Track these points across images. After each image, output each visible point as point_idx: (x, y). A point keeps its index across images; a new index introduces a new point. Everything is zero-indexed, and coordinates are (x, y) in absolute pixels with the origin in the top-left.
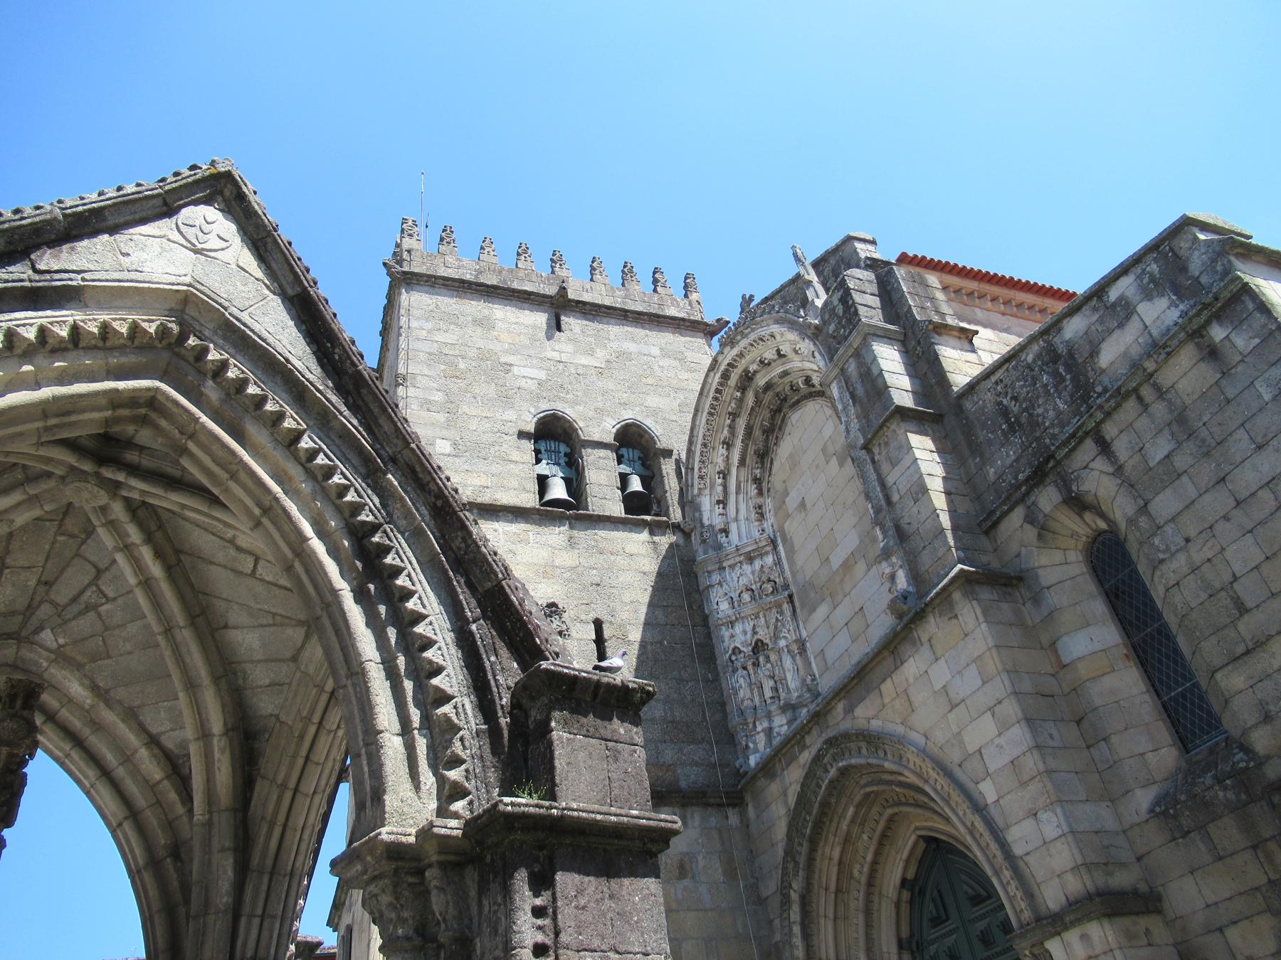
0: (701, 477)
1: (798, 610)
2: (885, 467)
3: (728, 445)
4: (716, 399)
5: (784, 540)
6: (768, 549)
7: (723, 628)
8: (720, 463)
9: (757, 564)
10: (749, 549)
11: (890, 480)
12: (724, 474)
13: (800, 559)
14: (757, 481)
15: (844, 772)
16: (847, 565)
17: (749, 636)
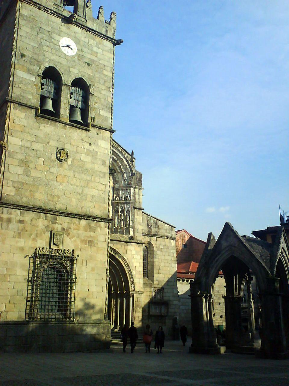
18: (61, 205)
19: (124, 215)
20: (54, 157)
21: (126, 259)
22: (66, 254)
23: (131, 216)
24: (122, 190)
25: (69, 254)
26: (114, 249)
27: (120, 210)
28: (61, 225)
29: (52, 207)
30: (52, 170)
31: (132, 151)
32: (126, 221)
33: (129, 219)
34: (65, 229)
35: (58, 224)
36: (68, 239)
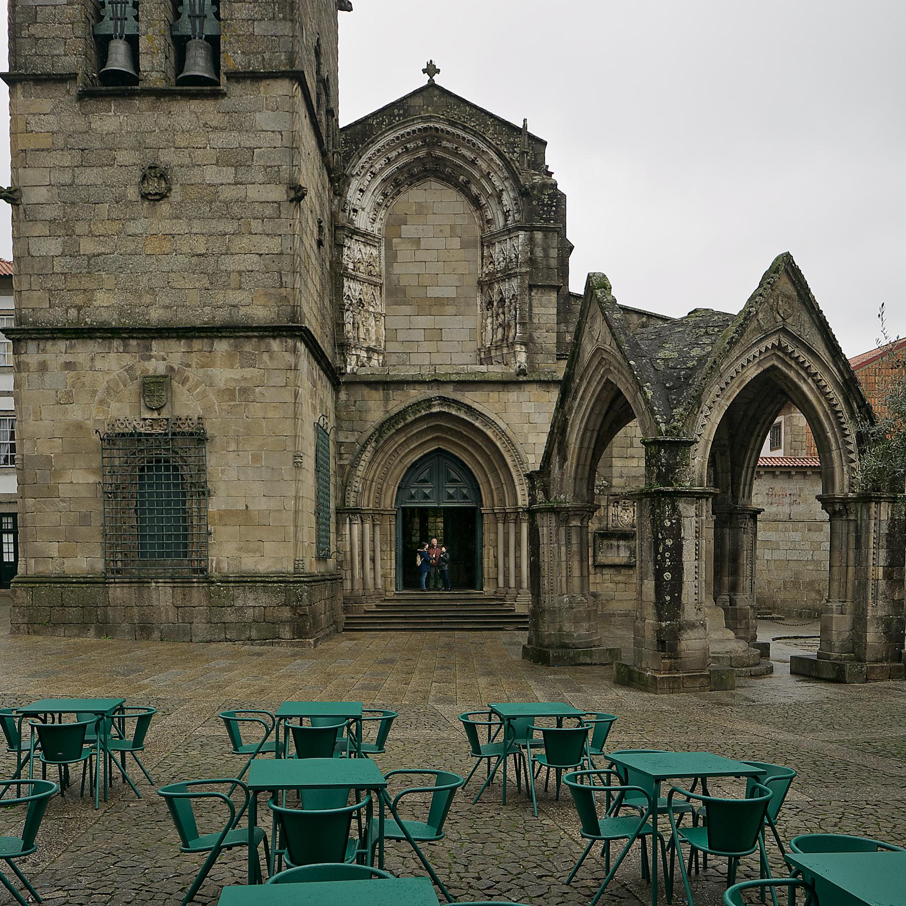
0: (363, 167)
1: (383, 296)
2: (535, 303)
3: (389, 162)
4: (408, 133)
5: (389, 246)
6: (376, 244)
7: (345, 279)
8: (378, 166)
9: (369, 250)
10: (369, 237)
11: (536, 311)
12: (374, 175)
13: (397, 269)
14: (385, 195)
15: (441, 413)
16: (440, 302)
17: (357, 294)
18: (161, 311)
19: (504, 313)
20: (132, 193)
21: (503, 426)
22: (179, 427)
23: (518, 312)
24: (499, 242)
25: (189, 426)
26: (468, 406)
27: (496, 298)
28: (164, 359)
29: (141, 322)
30: (134, 227)
31: (525, 120)
32: (509, 327)
33: (516, 319)
34: (176, 367)
35: (157, 360)
36: (185, 389)
